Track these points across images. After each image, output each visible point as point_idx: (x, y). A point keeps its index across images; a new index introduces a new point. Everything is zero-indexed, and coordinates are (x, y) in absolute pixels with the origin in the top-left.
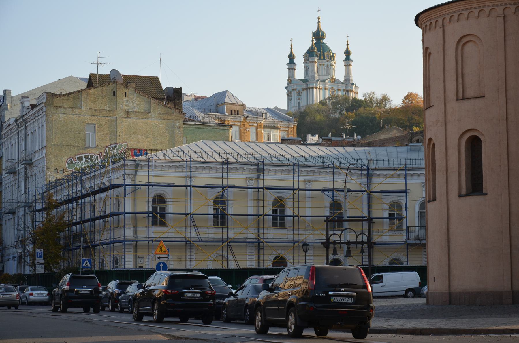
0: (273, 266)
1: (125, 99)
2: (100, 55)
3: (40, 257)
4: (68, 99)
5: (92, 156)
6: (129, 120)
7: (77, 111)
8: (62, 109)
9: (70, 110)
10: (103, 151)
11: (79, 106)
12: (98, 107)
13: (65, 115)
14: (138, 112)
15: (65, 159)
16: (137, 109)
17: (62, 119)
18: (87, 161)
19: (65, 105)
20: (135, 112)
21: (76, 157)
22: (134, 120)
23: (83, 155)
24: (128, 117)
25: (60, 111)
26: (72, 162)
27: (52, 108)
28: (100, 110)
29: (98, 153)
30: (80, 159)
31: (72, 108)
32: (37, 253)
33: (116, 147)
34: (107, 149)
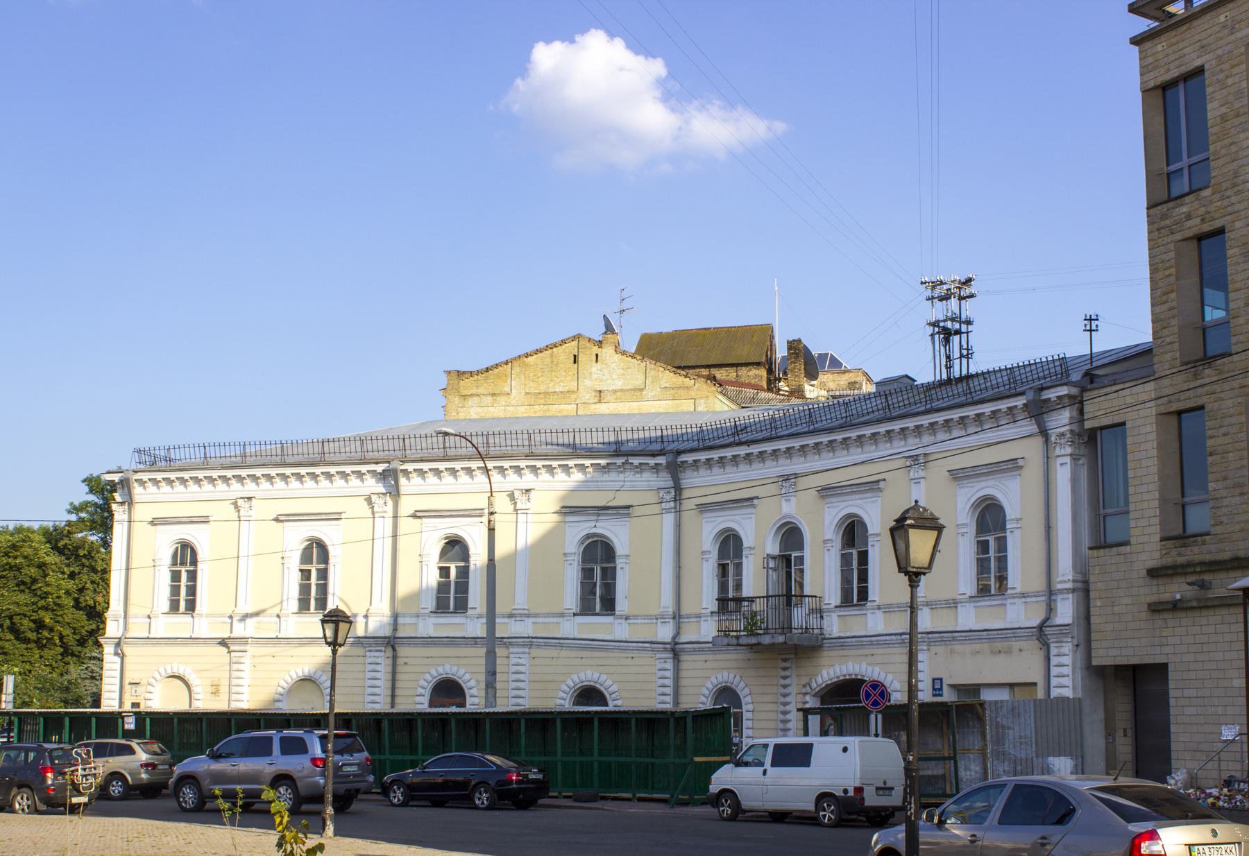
0: (431, 706)
1: (595, 368)
4: (486, 379)
7: (502, 400)
8: (475, 398)
9: (490, 398)
12: (543, 388)
13: (480, 410)
14: (622, 390)
16: (619, 384)
19: (480, 391)
20: (615, 391)
24: (600, 402)
28: (546, 394)
31: (493, 395)
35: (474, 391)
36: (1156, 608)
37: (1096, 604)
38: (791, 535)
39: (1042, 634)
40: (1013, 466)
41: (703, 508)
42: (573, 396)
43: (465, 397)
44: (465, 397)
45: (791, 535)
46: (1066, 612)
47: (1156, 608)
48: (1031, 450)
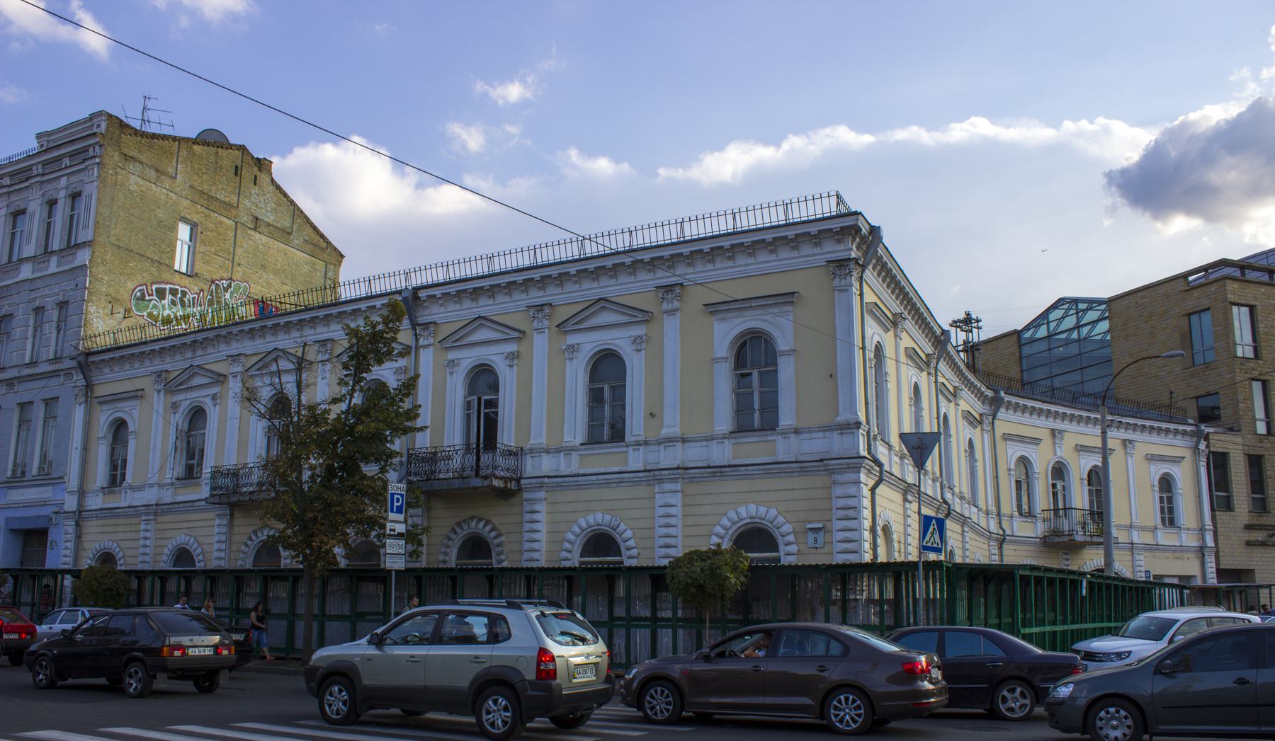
1: (255, 190)
2: (149, 104)
3: (399, 510)
4: (151, 147)
5: (184, 294)
6: (257, 236)
7: (167, 183)
9: (153, 174)
10: (206, 288)
11: (171, 171)
12: (205, 188)
13: (141, 182)
15: (131, 285)
16: (270, 218)
17: (133, 187)
18: (173, 303)
20: (269, 225)
21: (154, 287)
22: (265, 239)
23: (168, 287)
24: (255, 229)
25: (131, 166)
26: (143, 295)
27: (116, 154)
28: (210, 198)
29: (196, 289)
30: (161, 294)
31: (157, 170)
32: (393, 495)
33: (230, 286)
34: (213, 287)
35: (134, 153)
36: (1248, 543)
37: (1221, 538)
38: (1059, 471)
39: (1201, 551)
40: (1177, 460)
41: (1008, 437)
42: (234, 212)
43: (127, 157)
44: (127, 157)
45: (1059, 471)
46: (1210, 542)
47: (1248, 543)
48: (1187, 453)
